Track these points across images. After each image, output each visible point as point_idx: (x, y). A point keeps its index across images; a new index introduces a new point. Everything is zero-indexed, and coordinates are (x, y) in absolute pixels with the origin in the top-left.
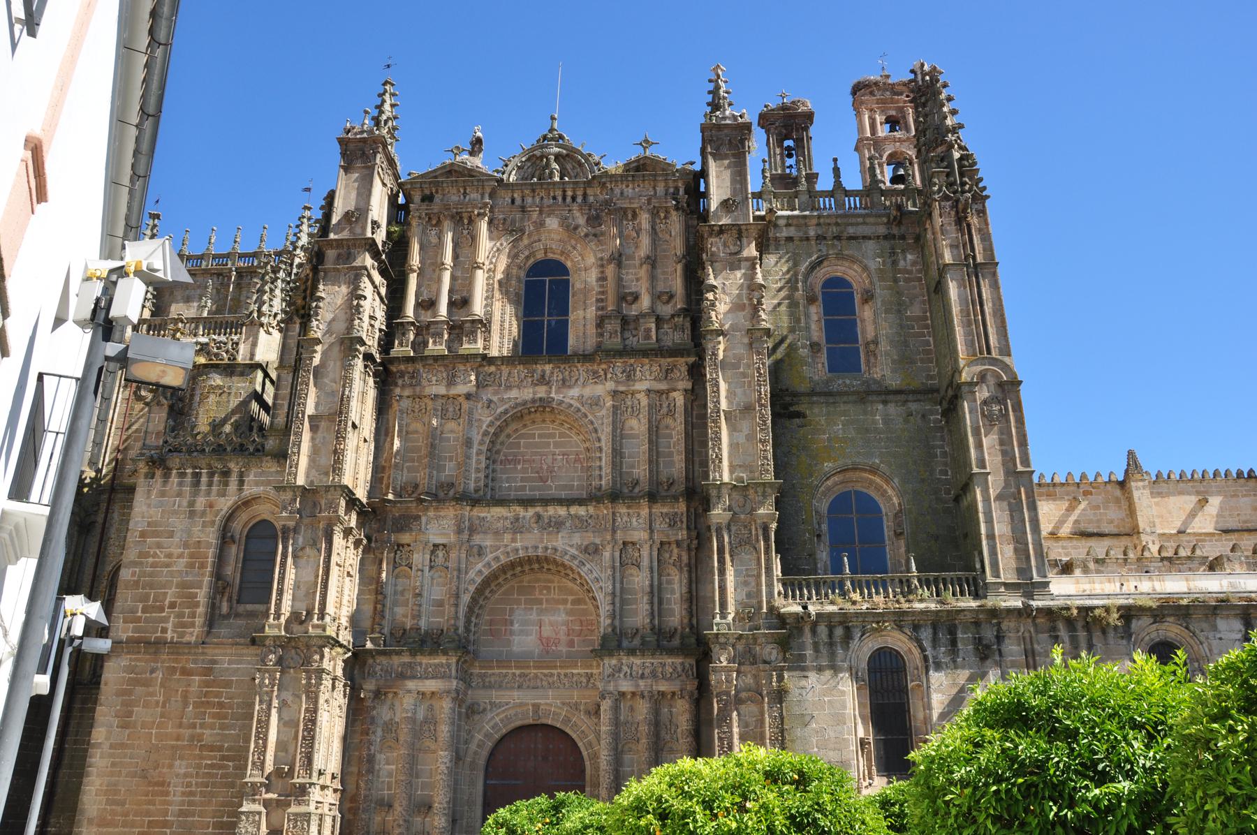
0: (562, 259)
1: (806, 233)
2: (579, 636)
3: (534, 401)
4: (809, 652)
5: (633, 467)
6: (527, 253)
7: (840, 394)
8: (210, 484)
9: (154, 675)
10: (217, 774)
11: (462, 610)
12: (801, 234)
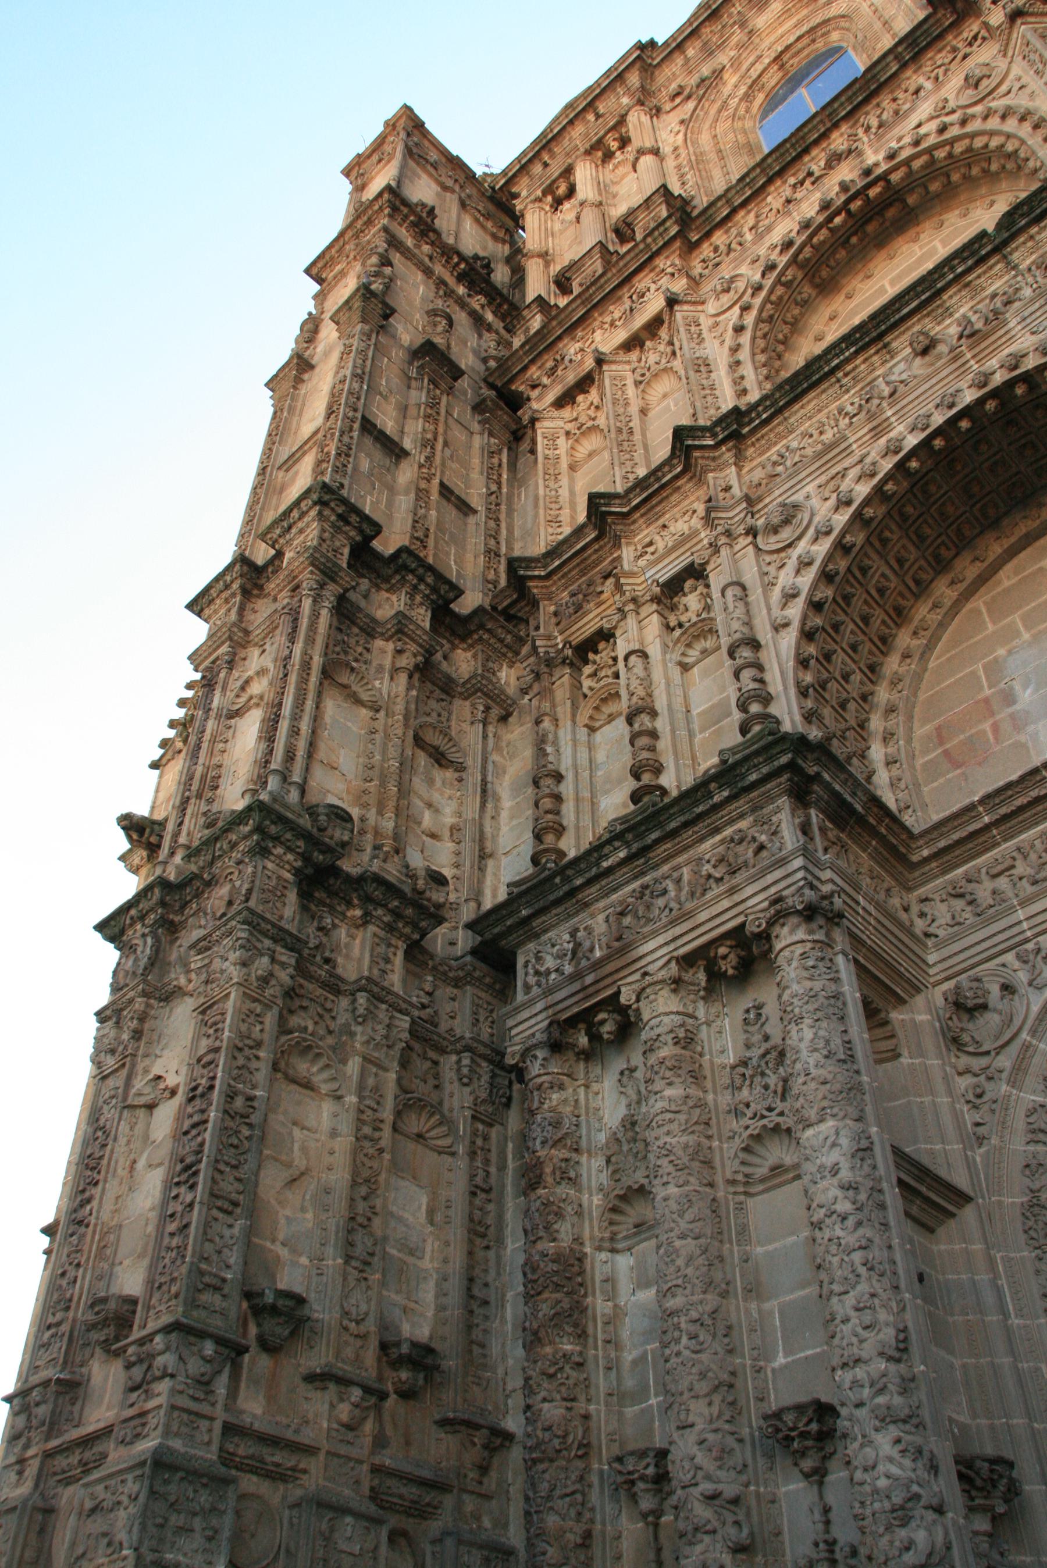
6: (743, 89)
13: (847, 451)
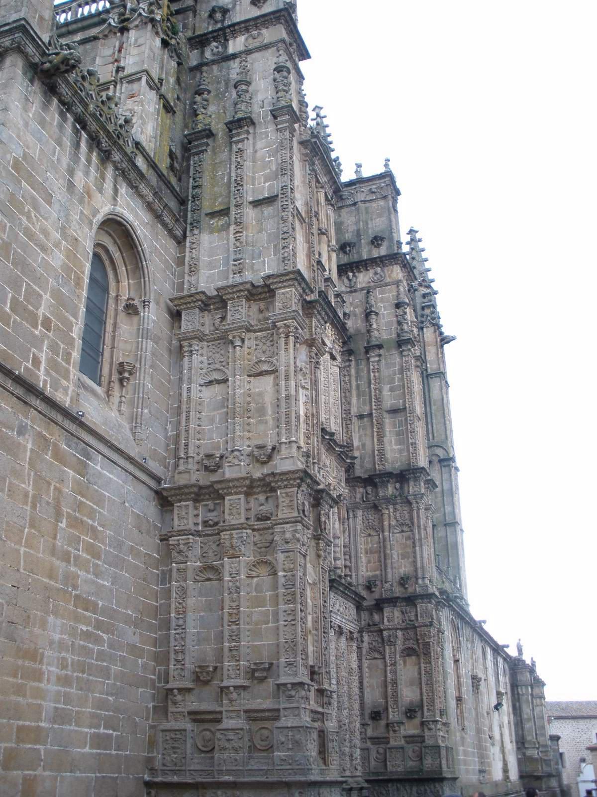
9: (21, 439)
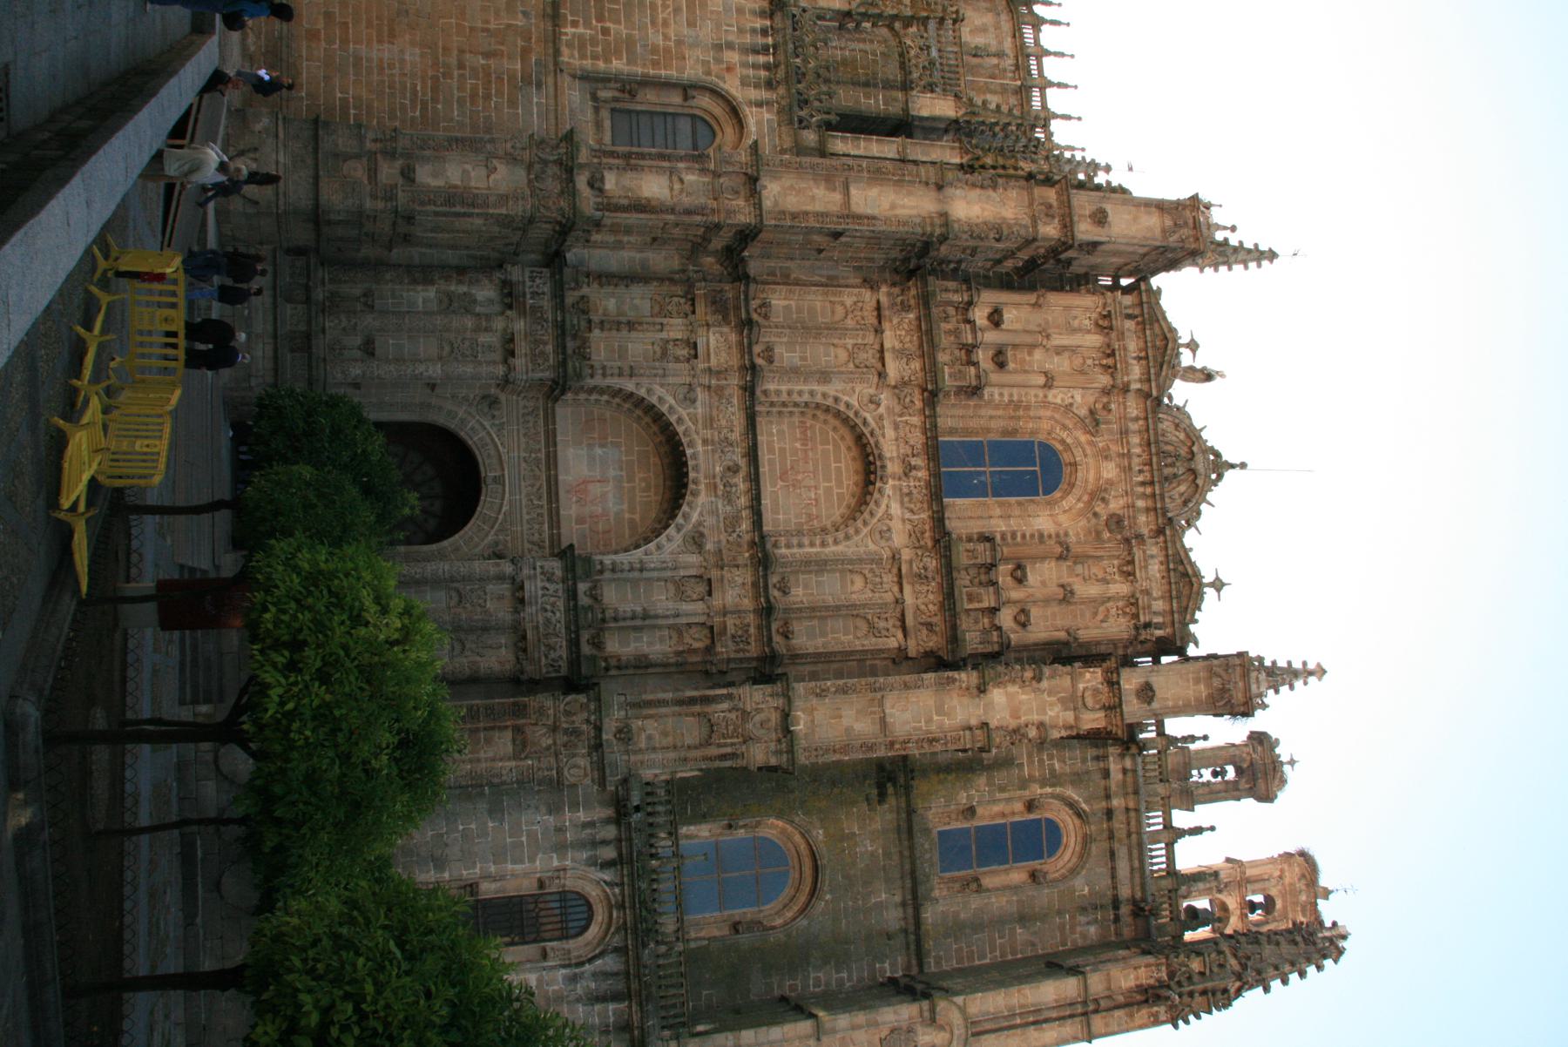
0: (1063, 486)
1: (1116, 794)
2: (591, 530)
3: (881, 457)
4: (582, 816)
5: (806, 587)
6: (1069, 441)
7: (911, 848)
8: (755, 66)
9: (520, 15)
10: (405, 98)
11: (615, 382)
12: (1113, 788)
13: (705, 427)
